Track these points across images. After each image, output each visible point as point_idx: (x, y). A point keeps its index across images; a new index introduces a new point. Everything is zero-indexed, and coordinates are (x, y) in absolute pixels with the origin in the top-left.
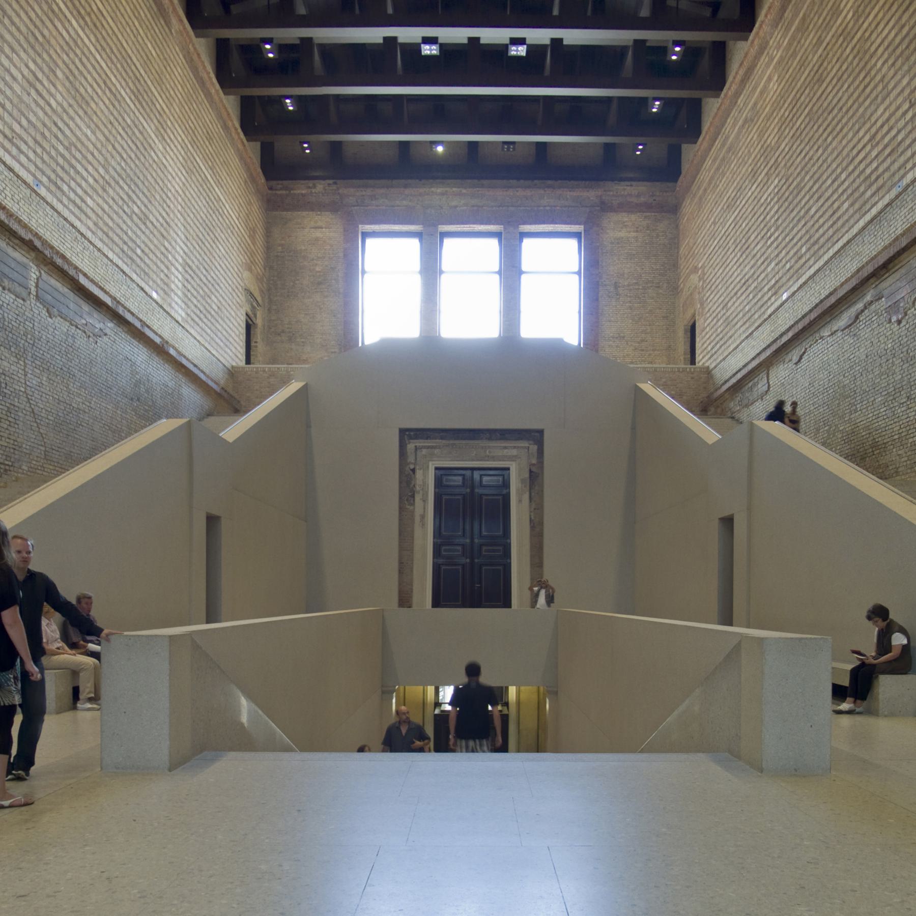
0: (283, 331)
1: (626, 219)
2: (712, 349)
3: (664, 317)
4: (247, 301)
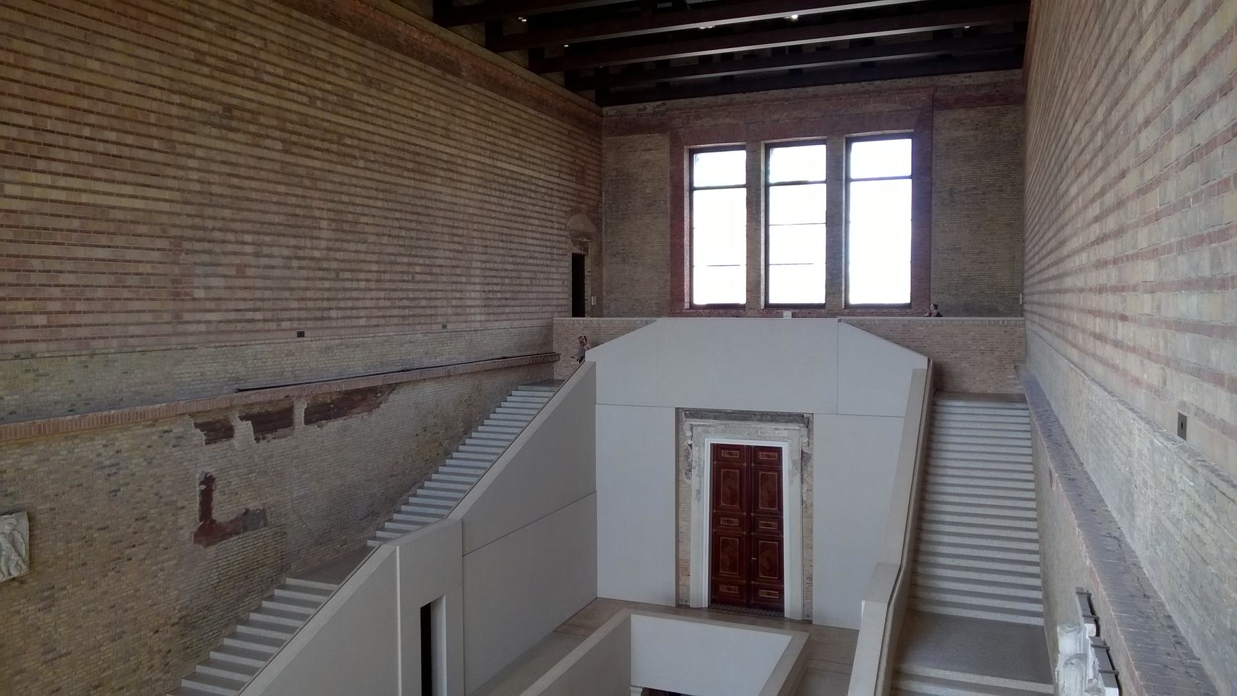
0: (618, 253)
1: (963, 116)
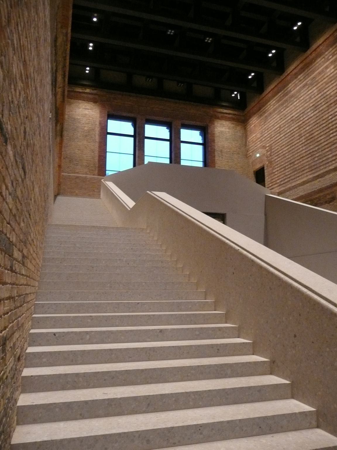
0: (67, 157)
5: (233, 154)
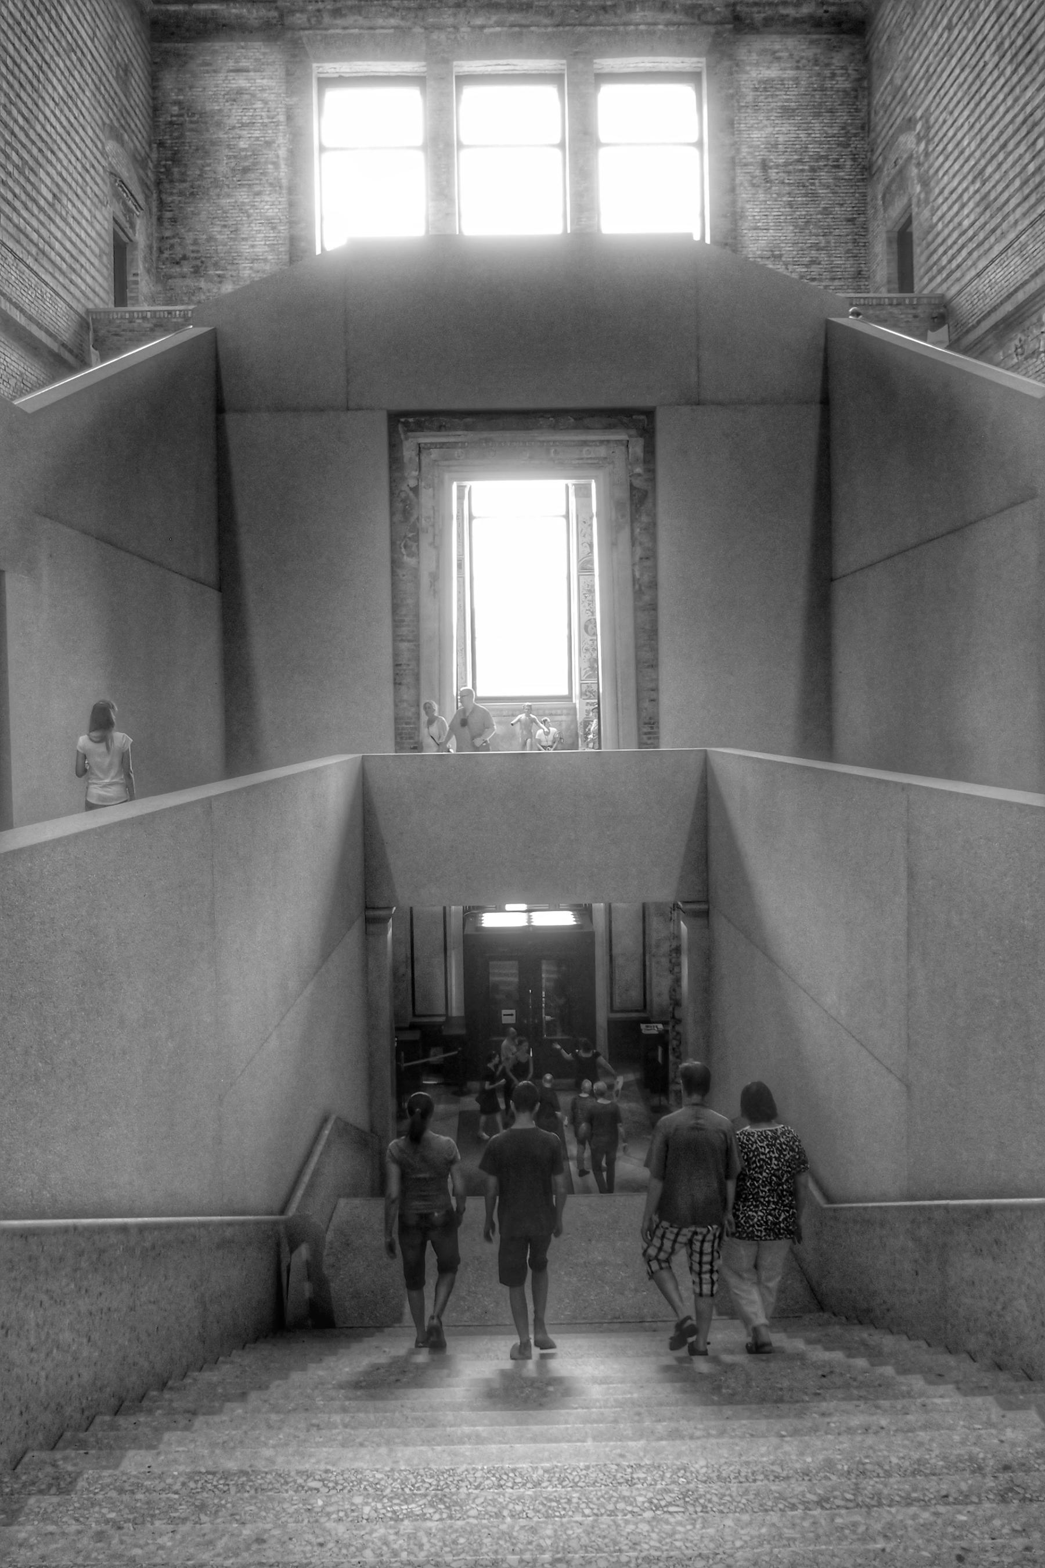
0: (184, 258)
1: (777, 47)
2: (950, 261)
3: (849, 220)
4: (116, 195)
5: (813, 170)
